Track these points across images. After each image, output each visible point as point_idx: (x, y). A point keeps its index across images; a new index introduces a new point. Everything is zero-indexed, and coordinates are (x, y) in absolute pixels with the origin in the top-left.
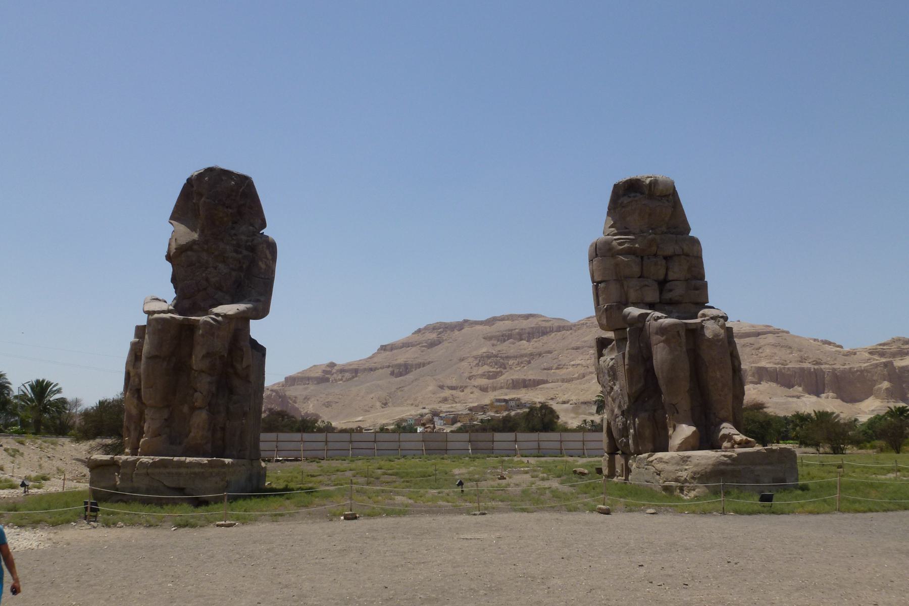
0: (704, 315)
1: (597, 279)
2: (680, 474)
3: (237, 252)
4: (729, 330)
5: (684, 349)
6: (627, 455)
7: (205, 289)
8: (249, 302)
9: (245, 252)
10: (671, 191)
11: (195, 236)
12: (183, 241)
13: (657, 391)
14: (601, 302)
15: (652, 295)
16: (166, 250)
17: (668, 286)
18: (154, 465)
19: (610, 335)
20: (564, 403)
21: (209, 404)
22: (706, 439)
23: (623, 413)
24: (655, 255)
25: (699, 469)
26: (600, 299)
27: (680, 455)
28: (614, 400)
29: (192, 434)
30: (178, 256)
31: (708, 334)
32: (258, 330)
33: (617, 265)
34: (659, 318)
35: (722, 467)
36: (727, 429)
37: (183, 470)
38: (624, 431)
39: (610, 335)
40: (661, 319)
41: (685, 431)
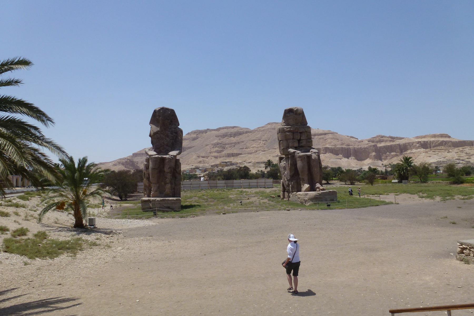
3: (172, 134)
6: (289, 192)
8: (177, 150)
9: (174, 134)
11: (159, 129)
12: (155, 131)
13: (298, 175)
15: (296, 145)
17: (301, 141)
19: (284, 156)
20: (249, 163)
22: (312, 188)
23: (288, 180)
24: (297, 132)
27: (305, 193)
29: (166, 191)
30: (153, 136)
31: (313, 158)
33: (286, 135)
36: (318, 185)
38: (288, 186)
39: (284, 156)
40: (299, 153)
41: (307, 186)
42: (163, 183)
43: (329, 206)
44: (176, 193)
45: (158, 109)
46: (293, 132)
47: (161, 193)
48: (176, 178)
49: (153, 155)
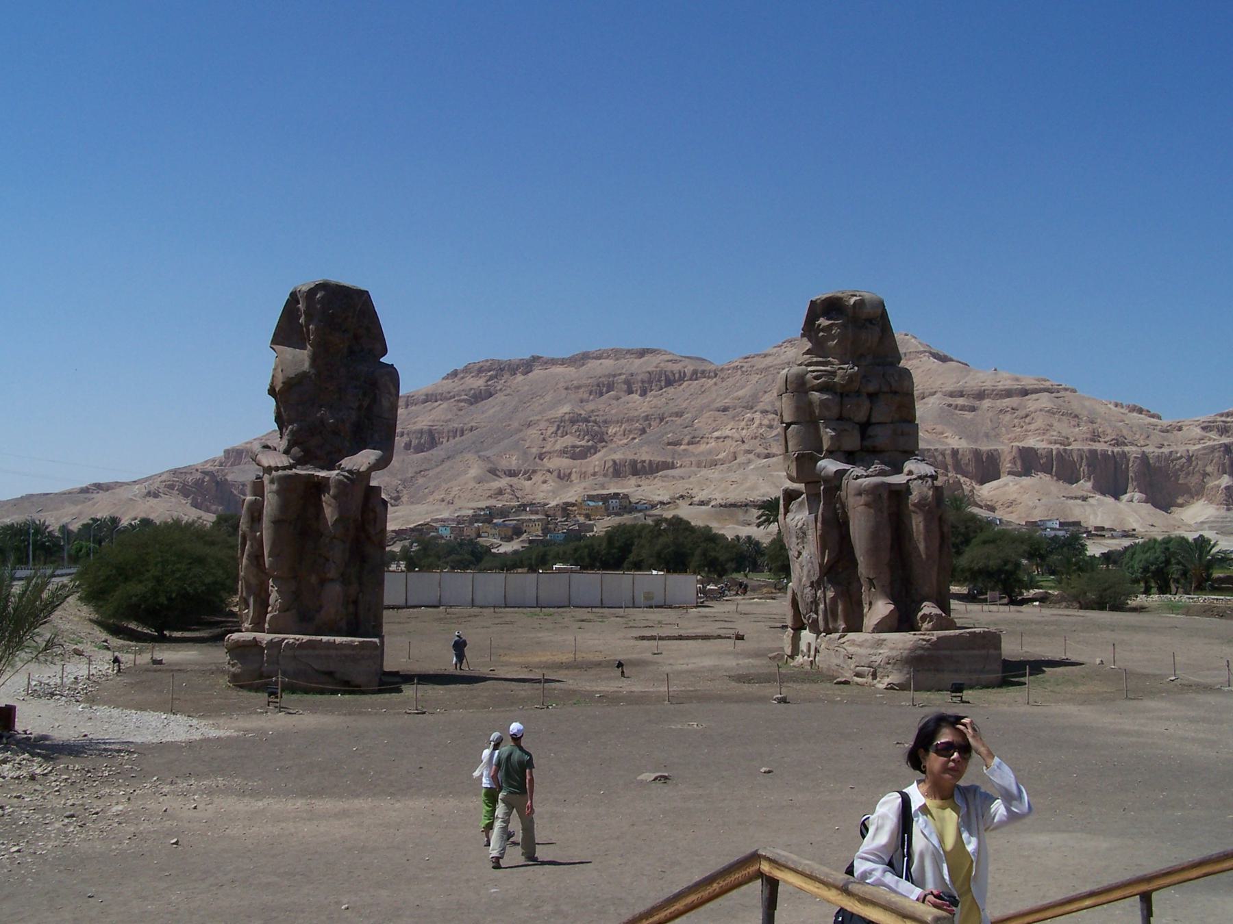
1: (787, 419)
2: (873, 658)
5: (886, 514)
10: (880, 311)
14: (790, 449)
15: (852, 441)
16: (269, 382)
17: (872, 431)
18: (302, 645)
21: (342, 575)
22: (903, 621)
23: (812, 585)
24: (858, 393)
25: (894, 653)
26: (790, 444)
28: (802, 567)
34: (858, 477)
35: (920, 652)
36: (929, 608)
37: (333, 652)
39: (801, 486)
40: (861, 478)
41: (881, 608)
42: (314, 579)
44: (364, 618)
45: (305, 289)
46: (841, 393)
47: (303, 614)
49: (277, 469)
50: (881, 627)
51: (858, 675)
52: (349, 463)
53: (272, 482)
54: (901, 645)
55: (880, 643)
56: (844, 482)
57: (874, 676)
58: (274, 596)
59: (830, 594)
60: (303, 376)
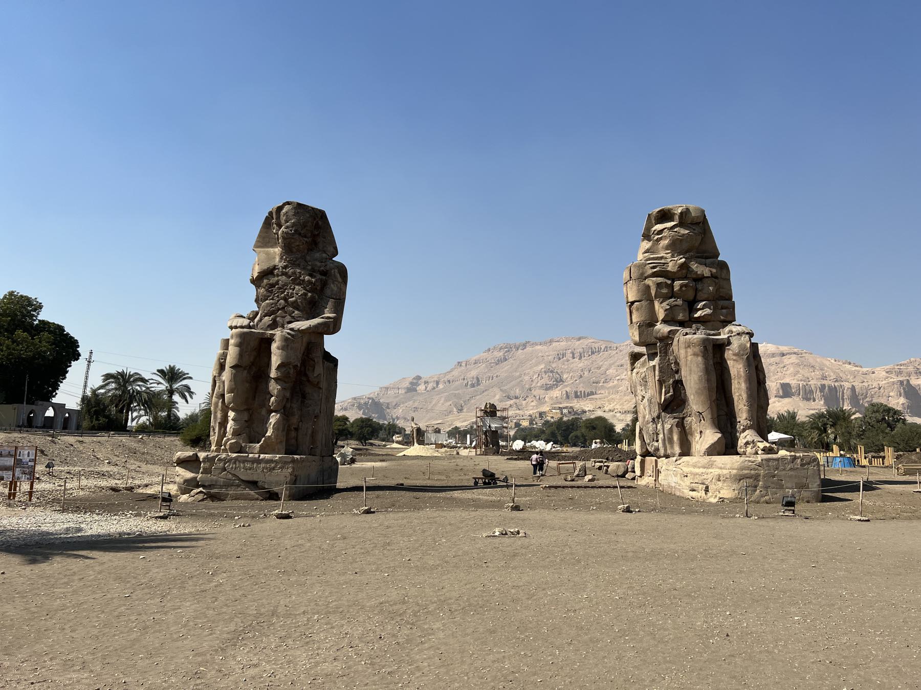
0: (731, 332)
1: (631, 300)
2: (705, 477)
4: (754, 346)
5: (711, 362)
7: (283, 308)
9: (319, 276)
14: (634, 321)
21: (284, 407)
26: (634, 317)
32: (331, 343)
34: (687, 334)
35: (746, 472)
39: (643, 350)
43: (790, 504)
48: (304, 396)
49: (236, 327)
50: (713, 451)
51: (694, 490)
52: (296, 325)
53: (232, 337)
54: (728, 466)
55: (710, 465)
56: (676, 340)
57: (707, 490)
58: (230, 425)
59: (667, 426)
60: (275, 268)
